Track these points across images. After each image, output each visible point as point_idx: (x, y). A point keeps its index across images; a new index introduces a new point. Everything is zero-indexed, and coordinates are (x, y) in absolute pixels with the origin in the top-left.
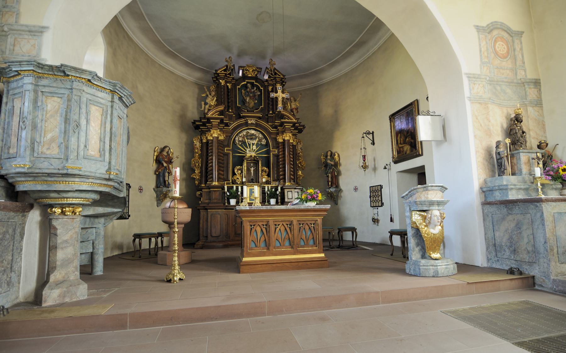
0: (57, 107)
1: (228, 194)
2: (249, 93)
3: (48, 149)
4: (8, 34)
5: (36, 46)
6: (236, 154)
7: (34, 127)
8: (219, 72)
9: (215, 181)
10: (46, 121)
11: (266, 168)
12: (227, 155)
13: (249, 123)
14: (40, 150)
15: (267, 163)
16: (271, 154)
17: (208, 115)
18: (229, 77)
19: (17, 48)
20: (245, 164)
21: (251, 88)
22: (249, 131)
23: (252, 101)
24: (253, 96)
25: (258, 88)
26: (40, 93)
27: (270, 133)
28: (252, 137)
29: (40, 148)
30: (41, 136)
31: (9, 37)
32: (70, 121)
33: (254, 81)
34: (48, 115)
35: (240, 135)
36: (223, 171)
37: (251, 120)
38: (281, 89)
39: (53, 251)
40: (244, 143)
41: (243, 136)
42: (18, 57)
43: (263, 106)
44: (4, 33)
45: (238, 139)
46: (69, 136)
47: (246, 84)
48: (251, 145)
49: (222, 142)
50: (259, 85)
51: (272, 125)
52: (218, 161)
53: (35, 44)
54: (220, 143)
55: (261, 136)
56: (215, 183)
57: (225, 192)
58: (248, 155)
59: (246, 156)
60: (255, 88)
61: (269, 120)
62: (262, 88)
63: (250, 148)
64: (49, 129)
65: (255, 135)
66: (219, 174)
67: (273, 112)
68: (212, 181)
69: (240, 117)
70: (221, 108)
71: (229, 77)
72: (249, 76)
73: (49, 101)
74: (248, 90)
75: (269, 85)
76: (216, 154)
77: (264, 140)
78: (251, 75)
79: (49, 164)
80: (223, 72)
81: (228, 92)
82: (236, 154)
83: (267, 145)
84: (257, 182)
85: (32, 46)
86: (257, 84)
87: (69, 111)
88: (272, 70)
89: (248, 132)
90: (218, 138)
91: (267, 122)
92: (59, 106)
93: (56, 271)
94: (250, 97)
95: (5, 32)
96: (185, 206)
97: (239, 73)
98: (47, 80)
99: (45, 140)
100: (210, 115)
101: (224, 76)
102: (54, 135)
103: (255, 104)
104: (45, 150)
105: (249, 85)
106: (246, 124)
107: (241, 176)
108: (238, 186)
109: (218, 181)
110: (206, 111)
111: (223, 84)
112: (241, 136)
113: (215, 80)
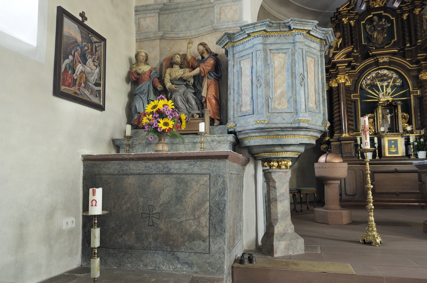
0: (282, 62)
3: (279, 104)
4: (214, 5)
5: (238, 12)
6: (366, 100)
7: (267, 84)
8: (341, 9)
9: (345, 133)
10: (275, 78)
11: (406, 113)
12: (355, 102)
13: (379, 62)
14: (273, 106)
15: (406, 108)
16: (412, 96)
17: (334, 59)
18: (352, 13)
19: (223, 16)
20: (380, 111)
21: (378, 20)
22: (379, 72)
23: (380, 36)
24: (381, 30)
25: (387, 18)
26: (268, 51)
27: (408, 71)
28: (382, 78)
29: (273, 104)
30: (272, 93)
31: (215, 7)
32: (295, 75)
34: (276, 72)
35: (368, 78)
36: (352, 121)
37: (383, 58)
39: (273, 203)
40: (373, 87)
41: (371, 78)
42: (224, 24)
43: (396, 39)
44: (211, 5)
45: (366, 83)
46: (296, 90)
47: (372, 17)
48: (385, 87)
49: (349, 88)
50: (389, 15)
51: (412, 60)
52: (347, 110)
53: (237, 9)
54: (347, 89)
55: (395, 76)
56: (345, 135)
58: (383, 99)
59: (380, 101)
60: (384, 20)
61: (406, 55)
62: (394, 18)
63: (383, 91)
64: (278, 84)
65: (387, 76)
66: (349, 124)
67: (411, 43)
68: (342, 133)
69: (367, 56)
70: (349, 49)
71: (352, 13)
72: (376, 6)
73: (276, 58)
74: (375, 23)
75: (403, 13)
76: (345, 103)
77: (399, 80)
78: (379, 5)
79: (282, 119)
80: (345, 9)
81: (351, 31)
82: (366, 100)
83: (404, 85)
84: (396, 132)
85: (234, 11)
86: (387, 14)
87: (294, 65)
89: (379, 73)
90: (345, 83)
91: (404, 57)
92: (285, 61)
93: (278, 223)
94: (379, 32)
95: (212, 3)
96: (341, 160)
97: (361, 6)
98: (272, 38)
99: (276, 96)
100: (336, 59)
101: (347, 12)
102: (282, 90)
103: (384, 38)
104: (277, 106)
105: (375, 17)
106: (377, 63)
108: (374, 137)
109: (348, 133)
110: (331, 56)
111: (345, 23)
112: (370, 79)
113: (334, 20)
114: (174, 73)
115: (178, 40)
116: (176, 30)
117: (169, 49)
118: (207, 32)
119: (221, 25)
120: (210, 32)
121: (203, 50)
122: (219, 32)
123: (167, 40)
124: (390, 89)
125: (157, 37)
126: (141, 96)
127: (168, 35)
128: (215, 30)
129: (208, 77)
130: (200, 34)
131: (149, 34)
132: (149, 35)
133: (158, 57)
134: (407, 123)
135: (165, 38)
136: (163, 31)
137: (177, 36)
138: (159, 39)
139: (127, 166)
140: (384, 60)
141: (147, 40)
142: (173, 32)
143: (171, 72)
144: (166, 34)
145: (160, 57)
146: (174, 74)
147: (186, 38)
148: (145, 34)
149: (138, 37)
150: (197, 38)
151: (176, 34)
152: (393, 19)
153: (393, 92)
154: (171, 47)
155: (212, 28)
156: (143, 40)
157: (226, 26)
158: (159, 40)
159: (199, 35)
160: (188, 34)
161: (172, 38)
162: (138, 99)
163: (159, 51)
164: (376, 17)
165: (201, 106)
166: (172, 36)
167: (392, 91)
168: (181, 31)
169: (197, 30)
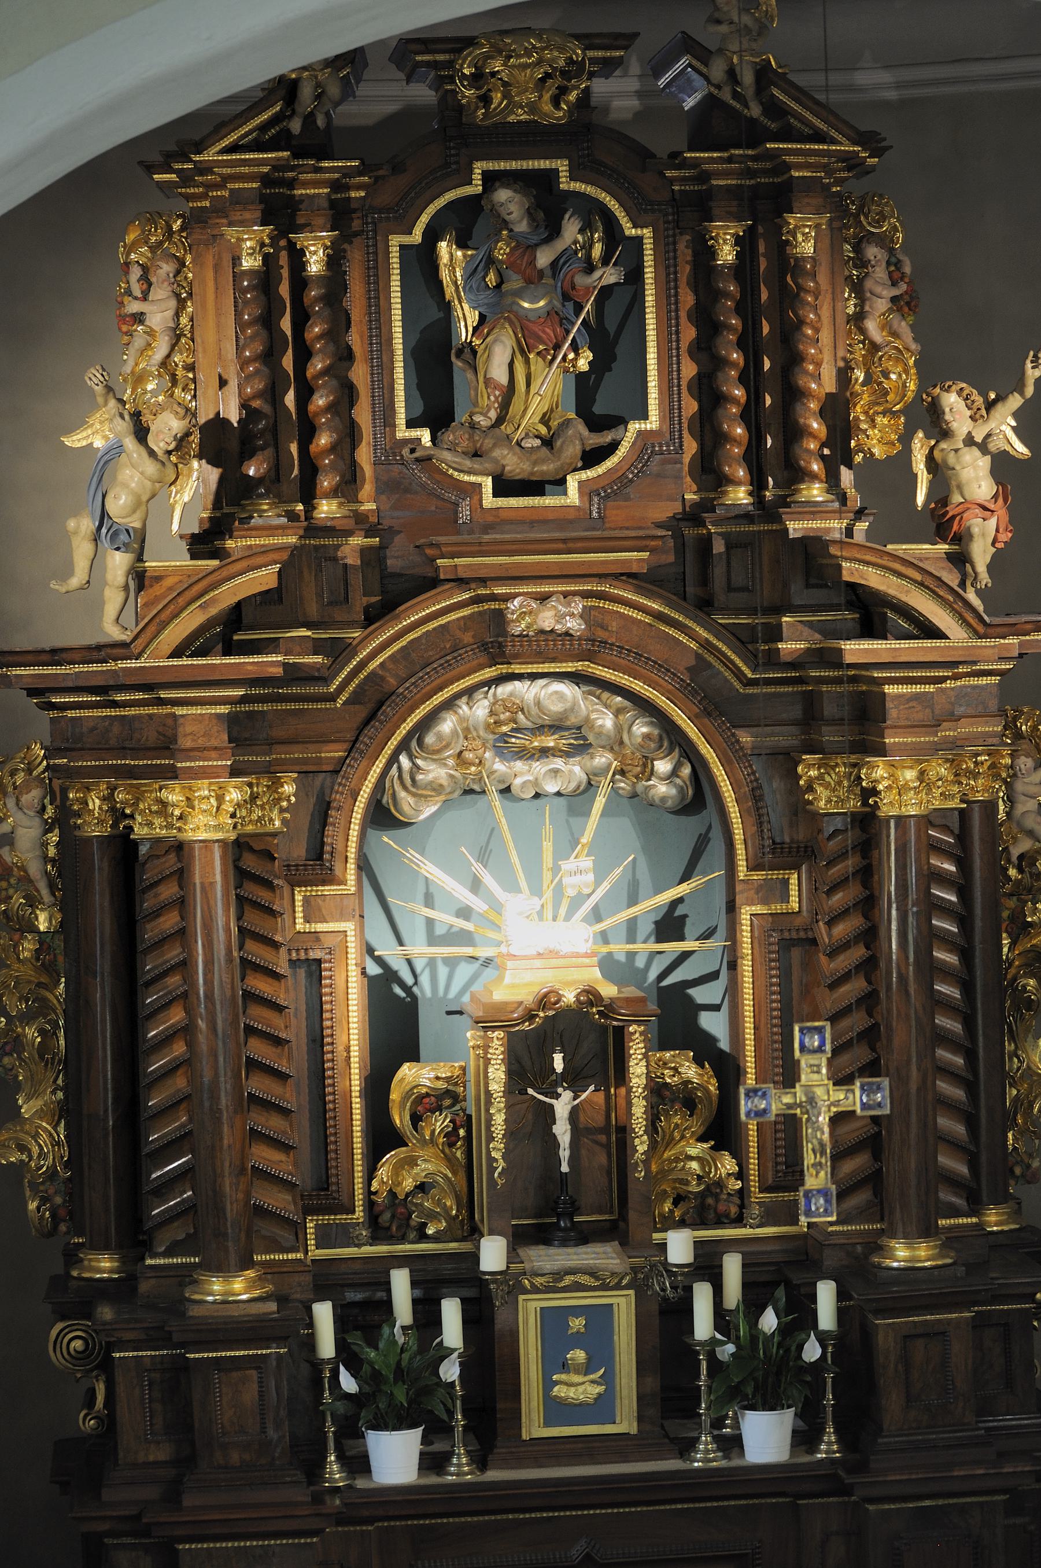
1: (348, 1383)
2: (515, 282)
33: (562, 166)
38: (808, 1195)
43: (653, 423)
50: (613, 204)
55: (641, 729)
57: (316, 1365)
60: (571, 231)
62: (647, 232)
74: (502, 251)
88: (748, 78)
105: (503, 195)
107: (450, 1161)
124: (587, 863)
134: (702, 1139)
140: (547, 620)
152: (640, 239)
153: (605, 886)
164: (518, 197)
167: (598, 883)
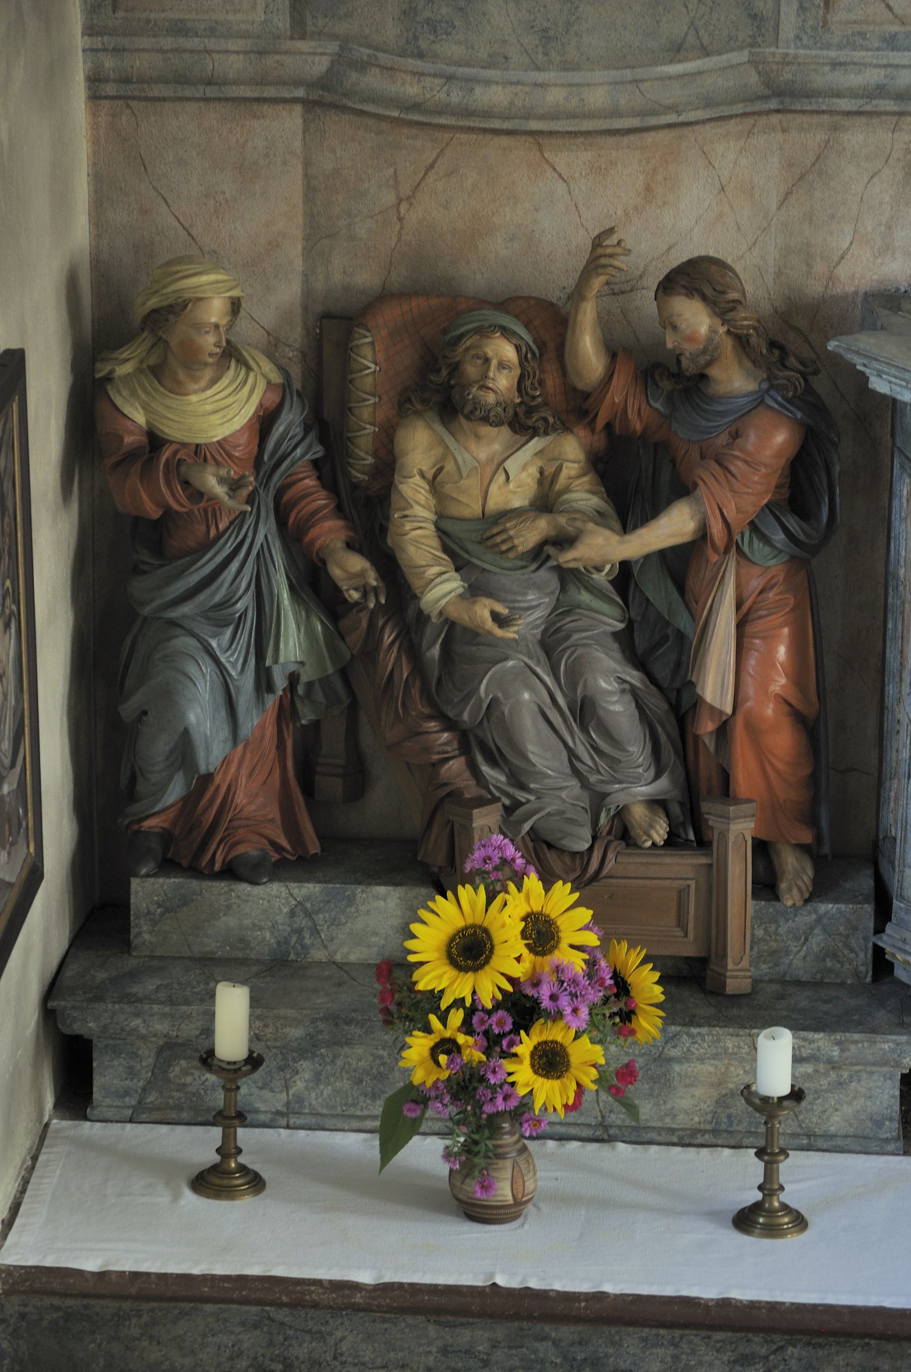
42: (858, 55)
114: (472, 484)
115: (463, 129)
116: (451, 49)
117: (388, 198)
118: (708, 103)
119: (835, 65)
120: (739, 108)
121: (709, 340)
122: (815, 119)
123: (371, 122)
125: (281, 82)
126: (214, 643)
127: (373, 80)
128: (779, 93)
129: (746, 549)
130: (654, 113)
131: (211, 43)
132: (208, 52)
133: (294, 252)
135: (350, 104)
136: (334, 37)
137: (456, 97)
138: (305, 102)
139: (321, 1336)
141: (188, 92)
142: (421, 56)
143: (449, 467)
144: (362, 66)
145: (308, 253)
146: (477, 492)
147: (534, 125)
148: (168, 42)
149: (109, 63)
150: (626, 140)
151: (450, 78)
154: (406, 190)
155: (753, 79)
156: (157, 91)
157: (872, 77)
158: (298, 109)
159: (641, 114)
160: (555, 96)
161: (416, 107)
162: (192, 669)
163: (298, 199)
165: (675, 733)
166: (411, 89)
168: (489, 66)
169: (628, 74)
